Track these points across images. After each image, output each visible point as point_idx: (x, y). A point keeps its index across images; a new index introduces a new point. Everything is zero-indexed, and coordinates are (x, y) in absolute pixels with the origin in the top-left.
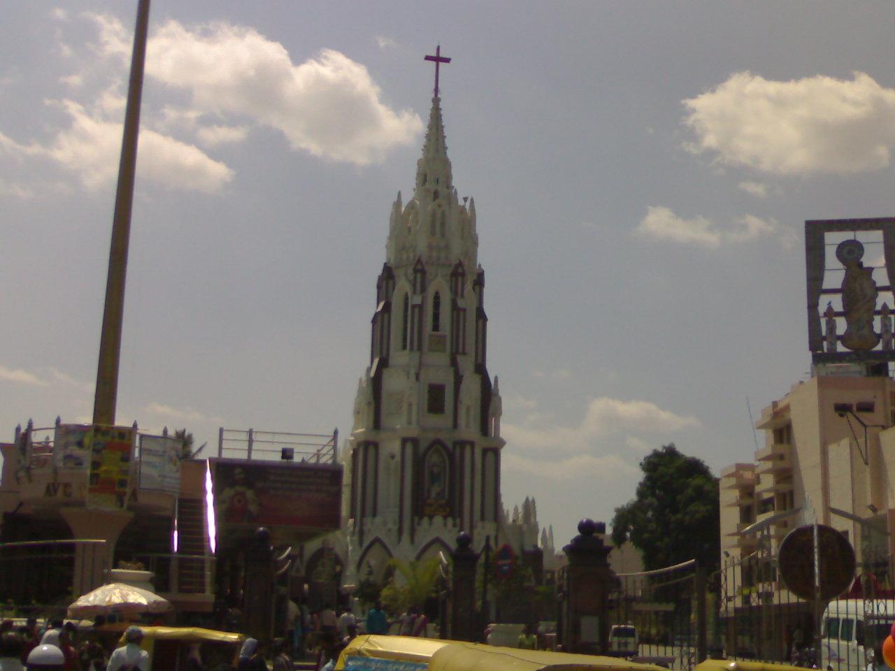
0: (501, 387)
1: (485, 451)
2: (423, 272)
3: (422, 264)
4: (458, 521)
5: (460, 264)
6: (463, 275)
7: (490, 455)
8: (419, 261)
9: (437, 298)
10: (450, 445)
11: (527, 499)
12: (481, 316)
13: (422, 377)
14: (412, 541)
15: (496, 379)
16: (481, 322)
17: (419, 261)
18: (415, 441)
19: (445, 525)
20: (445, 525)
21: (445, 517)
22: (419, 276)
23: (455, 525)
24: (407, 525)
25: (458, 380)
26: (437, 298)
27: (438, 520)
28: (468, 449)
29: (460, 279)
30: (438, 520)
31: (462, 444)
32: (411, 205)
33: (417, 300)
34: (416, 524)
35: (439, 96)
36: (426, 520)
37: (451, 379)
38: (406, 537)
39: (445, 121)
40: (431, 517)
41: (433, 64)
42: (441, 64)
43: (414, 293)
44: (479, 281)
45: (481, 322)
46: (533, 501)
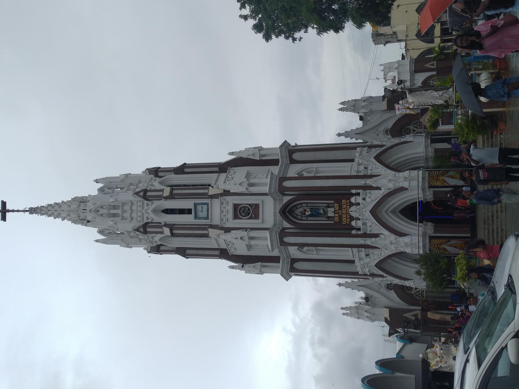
0: (237, 149)
1: (293, 161)
3: (139, 227)
4: (354, 191)
5: (137, 194)
6: (145, 191)
7: (296, 156)
8: (137, 230)
9: (168, 211)
11: (341, 109)
12: (182, 169)
13: (228, 225)
14: (376, 236)
15: (232, 154)
16: (186, 170)
17: (137, 230)
18: (283, 233)
19: (358, 204)
20: (358, 204)
21: (352, 204)
22: (149, 230)
23: (358, 194)
24: (360, 241)
25: (227, 193)
26: (168, 211)
27: (354, 211)
28: (287, 184)
29: (149, 194)
30: (354, 211)
31: (283, 191)
32: (101, 232)
33: (167, 231)
34: (359, 232)
35: (28, 209)
36: (353, 223)
37: (228, 198)
39: (44, 203)
40: (352, 218)
41: (8, 214)
42: (8, 207)
43: (162, 233)
44: (156, 172)
45: (186, 170)
46: (342, 103)
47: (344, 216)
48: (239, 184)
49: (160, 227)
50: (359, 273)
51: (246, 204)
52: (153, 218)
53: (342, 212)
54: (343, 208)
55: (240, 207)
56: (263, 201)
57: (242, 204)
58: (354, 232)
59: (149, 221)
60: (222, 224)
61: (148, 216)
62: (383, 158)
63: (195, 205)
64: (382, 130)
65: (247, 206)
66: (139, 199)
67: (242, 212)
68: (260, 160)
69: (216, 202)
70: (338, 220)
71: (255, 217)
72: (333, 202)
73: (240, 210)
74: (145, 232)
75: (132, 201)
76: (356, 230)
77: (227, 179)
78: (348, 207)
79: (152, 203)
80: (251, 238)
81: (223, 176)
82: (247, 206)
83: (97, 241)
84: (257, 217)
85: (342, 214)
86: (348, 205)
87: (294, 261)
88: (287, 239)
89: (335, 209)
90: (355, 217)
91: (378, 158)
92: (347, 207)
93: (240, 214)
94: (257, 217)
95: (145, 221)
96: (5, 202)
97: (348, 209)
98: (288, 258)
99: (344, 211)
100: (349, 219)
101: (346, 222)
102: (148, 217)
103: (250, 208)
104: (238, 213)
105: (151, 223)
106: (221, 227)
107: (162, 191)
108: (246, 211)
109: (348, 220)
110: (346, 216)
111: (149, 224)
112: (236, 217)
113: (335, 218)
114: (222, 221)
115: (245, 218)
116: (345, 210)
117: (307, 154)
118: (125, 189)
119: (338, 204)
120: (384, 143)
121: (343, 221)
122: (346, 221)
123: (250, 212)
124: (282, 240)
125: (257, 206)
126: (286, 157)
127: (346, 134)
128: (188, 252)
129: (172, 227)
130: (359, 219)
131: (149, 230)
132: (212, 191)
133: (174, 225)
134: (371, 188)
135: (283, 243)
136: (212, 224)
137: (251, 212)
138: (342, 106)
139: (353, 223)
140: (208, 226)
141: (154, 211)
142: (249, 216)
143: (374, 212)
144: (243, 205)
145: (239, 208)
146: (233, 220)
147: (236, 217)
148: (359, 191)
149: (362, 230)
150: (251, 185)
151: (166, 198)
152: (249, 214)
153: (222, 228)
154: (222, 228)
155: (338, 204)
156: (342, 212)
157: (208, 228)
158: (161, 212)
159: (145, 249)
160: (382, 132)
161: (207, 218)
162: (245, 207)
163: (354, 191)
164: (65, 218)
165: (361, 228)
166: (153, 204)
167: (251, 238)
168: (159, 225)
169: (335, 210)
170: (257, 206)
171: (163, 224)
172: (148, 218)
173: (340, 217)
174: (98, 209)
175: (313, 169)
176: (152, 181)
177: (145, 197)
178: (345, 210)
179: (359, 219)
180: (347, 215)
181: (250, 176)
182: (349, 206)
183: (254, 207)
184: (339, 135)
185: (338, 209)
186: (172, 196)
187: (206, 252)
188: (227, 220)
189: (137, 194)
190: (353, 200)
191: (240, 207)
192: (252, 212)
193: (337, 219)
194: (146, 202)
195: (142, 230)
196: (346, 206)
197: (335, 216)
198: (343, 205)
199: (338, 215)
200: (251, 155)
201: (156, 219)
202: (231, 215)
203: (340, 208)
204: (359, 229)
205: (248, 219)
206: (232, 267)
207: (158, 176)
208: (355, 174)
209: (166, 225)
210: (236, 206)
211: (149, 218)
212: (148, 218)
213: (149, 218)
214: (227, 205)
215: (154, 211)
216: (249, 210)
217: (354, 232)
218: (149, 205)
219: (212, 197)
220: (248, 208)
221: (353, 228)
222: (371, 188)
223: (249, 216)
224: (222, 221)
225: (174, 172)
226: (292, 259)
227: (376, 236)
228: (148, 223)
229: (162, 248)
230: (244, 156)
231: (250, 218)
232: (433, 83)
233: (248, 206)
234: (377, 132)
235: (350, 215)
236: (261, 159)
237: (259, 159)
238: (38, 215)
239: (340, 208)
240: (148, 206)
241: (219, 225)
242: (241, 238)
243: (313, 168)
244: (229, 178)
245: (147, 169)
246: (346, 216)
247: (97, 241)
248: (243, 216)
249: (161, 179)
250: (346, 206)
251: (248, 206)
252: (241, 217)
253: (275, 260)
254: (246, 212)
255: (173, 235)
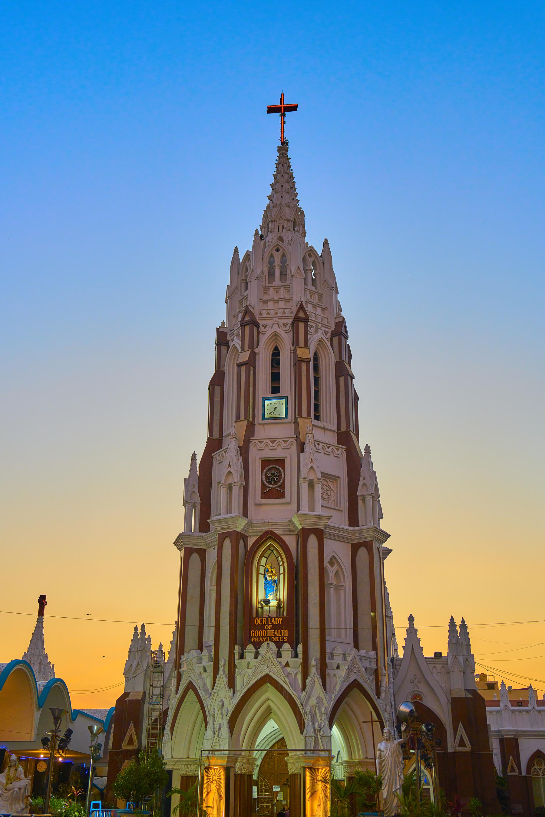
1: (355, 548)
2: (254, 324)
3: (252, 315)
4: (300, 647)
5: (301, 307)
6: (306, 320)
7: (362, 552)
9: (276, 353)
10: (291, 542)
14: (231, 684)
16: (342, 379)
17: (247, 312)
19: (279, 655)
20: (279, 655)
21: (279, 645)
22: (247, 328)
26: (276, 353)
28: (312, 541)
29: (301, 325)
32: (248, 256)
33: (245, 357)
34: (236, 657)
36: (250, 648)
37: (294, 448)
38: (222, 679)
40: (257, 645)
43: (243, 349)
45: (342, 379)
46: (464, 625)
47: (262, 633)
48: (312, 467)
49: (251, 346)
50: (182, 656)
51: (285, 477)
52: (265, 334)
53: (269, 629)
54: (275, 631)
55: (280, 468)
56: (289, 503)
57: (284, 471)
58: (237, 648)
59: (262, 329)
60: (254, 441)
61: (268, 327)
62: (356, 692)
63: (285, 397)
64: (419, 690)
65: (282, 479)
66: (295, 310)
67: (273, 472)
68: (357, 497)
69: (287, 431)
70: (257, 623)
71: (264, 492)
72: (285, 615)
73: (276, 468)
74: (243, 325)
75: (292, 300)
76: (241, 652)
77: (325, 445)
78: (277, 639)
79: (288, 331)
80: (230, 488)
81: (331, 438)
82: (282, 479)
83: (236, 251)
84: (265, 495)
85: (266, 631)
86: (279, 639)
87: (202, 553)
88: (227, 543)
89: (273, 619)
90: (259, 650)
91: (355, 685)
92: (276, 638)
93: (270, 468)
94: (265, 495)
95: (261, 323)
96: (296, 110)
97: (274, 639)
98: (207, 544)
99: (270, 632)
100: (258, 641)
101: (254, 636)
102: (267, 326)
103: (279, 484)
104: (271, 466)
105: (258, 333)
106: (249, 440)
107: (306, 345)
108: (274, 479)
109: (257, 640)
110: (263, 636)
111: (255, 329)
112: (265, 463)
113: (260, 619)
114: (259, 440)
115: (264, 476)
116: (272, 634)
117: (367, 571)
118: (313, 288)
119: (281, 623)
120: (383, 695)
121: (254, 631)
122: (255, 637)
123: (273, 485)
124: (227, 537)
125: (282, 495)
126: (360, 538)
127: (412, 632)
128: (218, 389)
129: (252, 362)
130: (256, 657)
131: (247, 328)
132: (305, 424)
133: (255, 368)
134: (305, 674)
135: (222, 537)
136: (255, 426)
137: (272, 486)
138: (458, 623)
139: (250, 648)
140: (251, 419)
141: (276, 335)
142: (266, 483)
143: (267, 679)
144: (283, 474)
145: (278, 467)
146: (260, 458)
147: (265, 463)
148: (300, 655)
149: (240, 661)
150: (311, 485)
151: (295, 352)
152: (270, 483)
153: (247, 442)
154: (247, 442)
155: (281, 623)
156: (269, 629)
157: (248, 421)
158: (275, 345)
159: (223, 323)
160: (416, 689)
161: (264, 418)
162: (279, 476)
163: (300, 647)
164: (271, 200)
165: (243, 661)
166: (285, 333)
167: (230, 488)
168: (254, 343)
169: (271, 618)
170: (282, 495)
171: (256, 350)
172: (265, 326)
173: (262, 627)
174: (281, 250)
175: (342, 581)
176: (323, 328)
177: (297, 320)
178: (272, 634)
179: (256, 657)
180: (264, 638)
181: (330, 480)
182: (278, 641)
183: (280, 491)
184: (411, 619)
185: (274, 623)
186: (298, 362)
187: (217, 418)
188: (260, 448)
189: (301, 307)
190: (286, 646)
191: (280, 468)
192: (272, 488)
193: (258, 622)
194: (290, 321)
195: (247, 318)
196: (277, 637)
197: (263, 619)
198: (279, 631)
199: (264, 624)
200: (364, 481)
201: (263, 339)
202: (269, 454)
203: (275, 627)
204: (242, 657)
205: (262, 481)
206: (194, 456)
207: (333, 337)
208: (328, 650)
209: (253, 356)
210: (281, 462)
211: (265, 328)
212: (265, 326)
213: (265, 328)
214: (283, 447)
215: (276, 335)
216: (276, 483)
217: (237, 648)
218: (286, 326)
219: (296, 423)
220: (279, 481)
221: (243, 647)
222: (305, 674)
223: (266, 483)
224: (259, 440)
225: (338, 360)
226: (205, 550)
227: (231, 684)
228: (257, 326)
229: (224, 348)
230: (363, 471)
231: (263, 486)
232: (540, 769)
233: (281, 481)
234: (416, 682)
235: (264, 642)
236: (359, 498)
237: (357, 494)
238: (276, 160)
239: (275, 627)
240: (284, 325)
241: (254, 437)
242: (230, 472)
243: (344, 582)
244: (326, 447)
245: (344, 319)
246: (263, 636)
247: (236, 251)
248: (266, 473)
249: (328, 343)
250: (277, 637)
251: (281, 481)
252: (265, 471)
253: (204, 526)
254: (272, 479)
255: (240, 365)
